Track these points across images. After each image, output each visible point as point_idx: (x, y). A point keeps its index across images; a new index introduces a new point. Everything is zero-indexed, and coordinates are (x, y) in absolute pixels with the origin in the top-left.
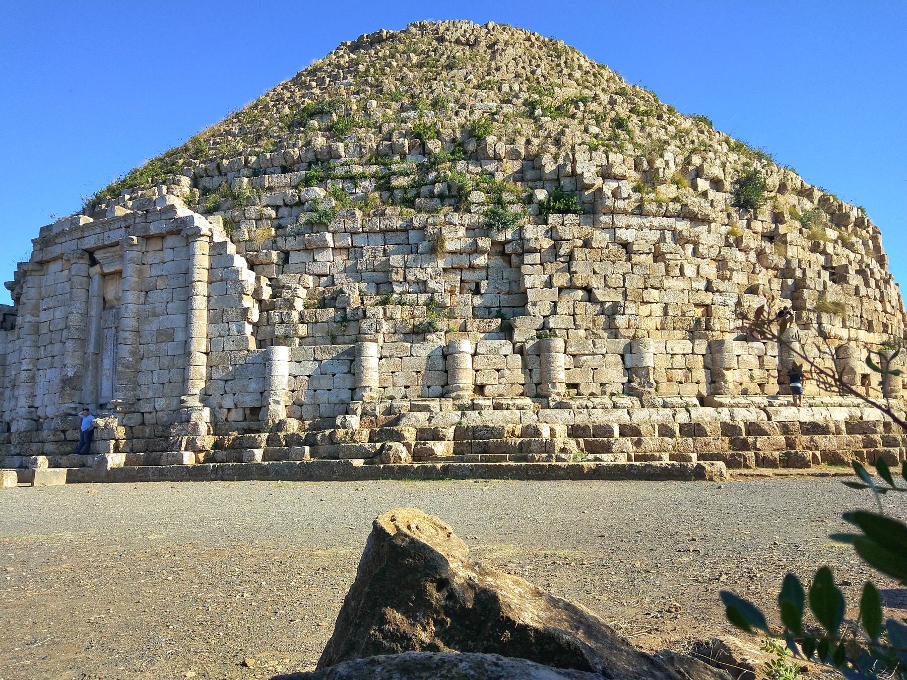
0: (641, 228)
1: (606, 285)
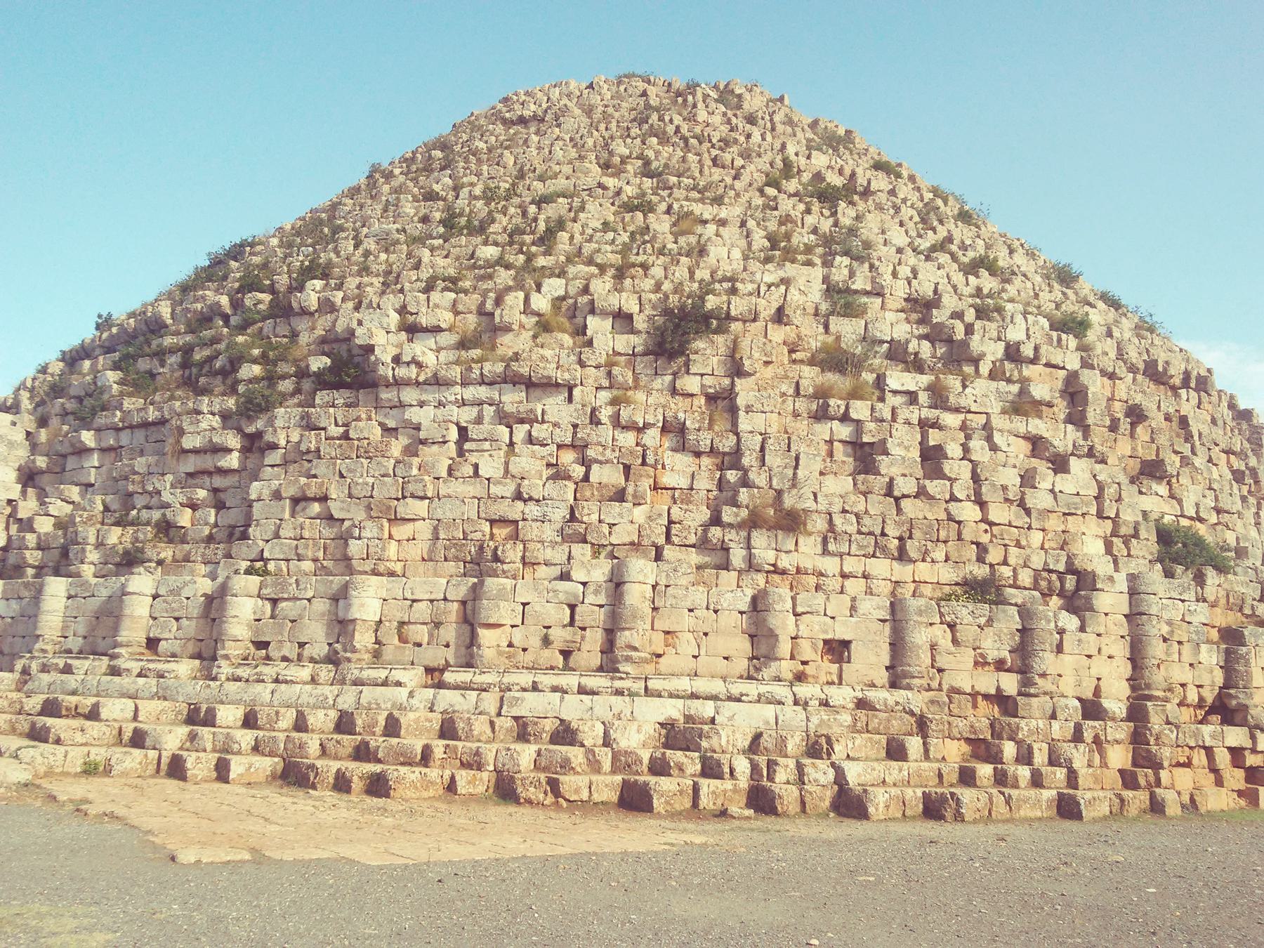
0: (441, 404)
1: (350, 496)
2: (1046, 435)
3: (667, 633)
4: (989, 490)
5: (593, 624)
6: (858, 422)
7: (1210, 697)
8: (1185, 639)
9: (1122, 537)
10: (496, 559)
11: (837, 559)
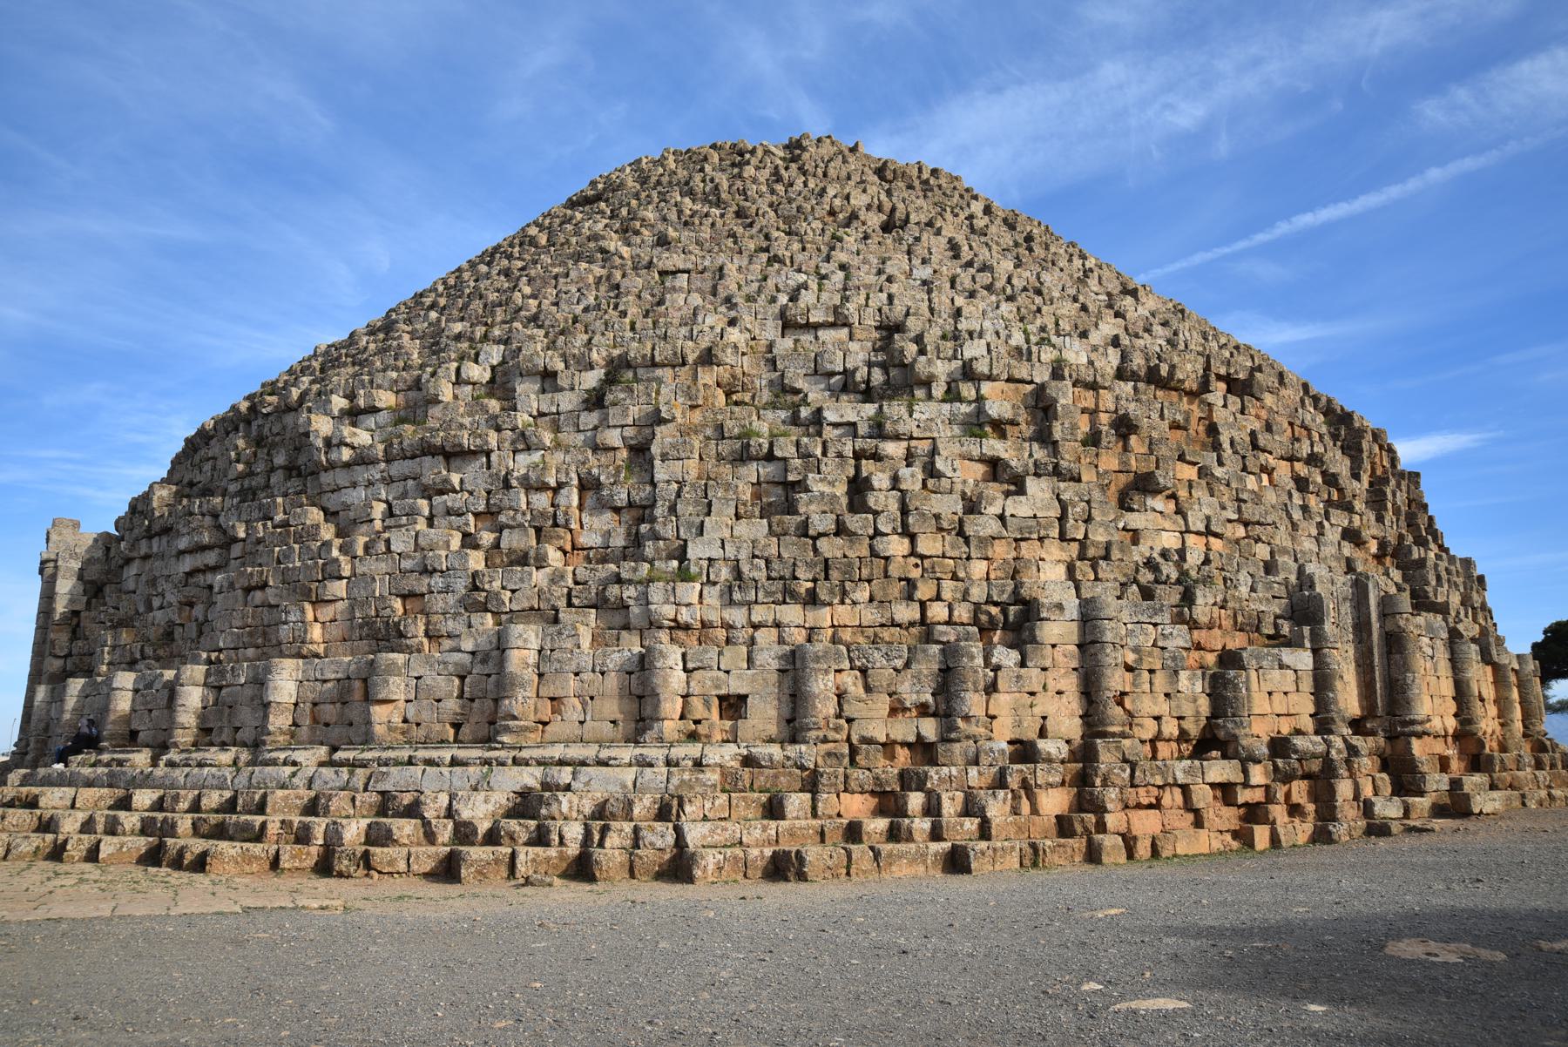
2: (1004, 455)
3: (552, 699)
4: (917, 520)
5: (480, 694)
6: (785, 459)
7: (1194, 730)
8: (1158, 666)
9: (1089, 560)
10: (401, 635)
11: (744, 610)
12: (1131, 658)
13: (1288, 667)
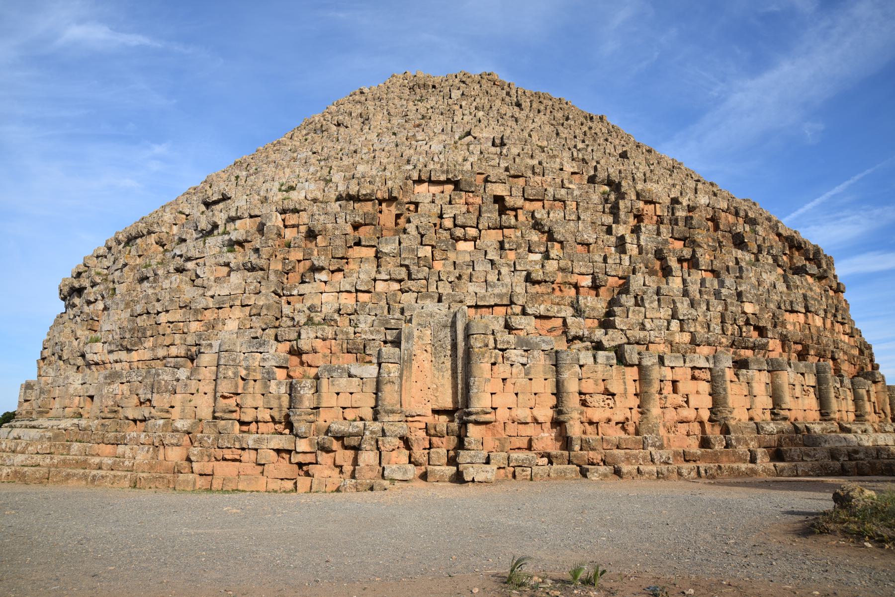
12: (243, 373)
13: (356, 376)
